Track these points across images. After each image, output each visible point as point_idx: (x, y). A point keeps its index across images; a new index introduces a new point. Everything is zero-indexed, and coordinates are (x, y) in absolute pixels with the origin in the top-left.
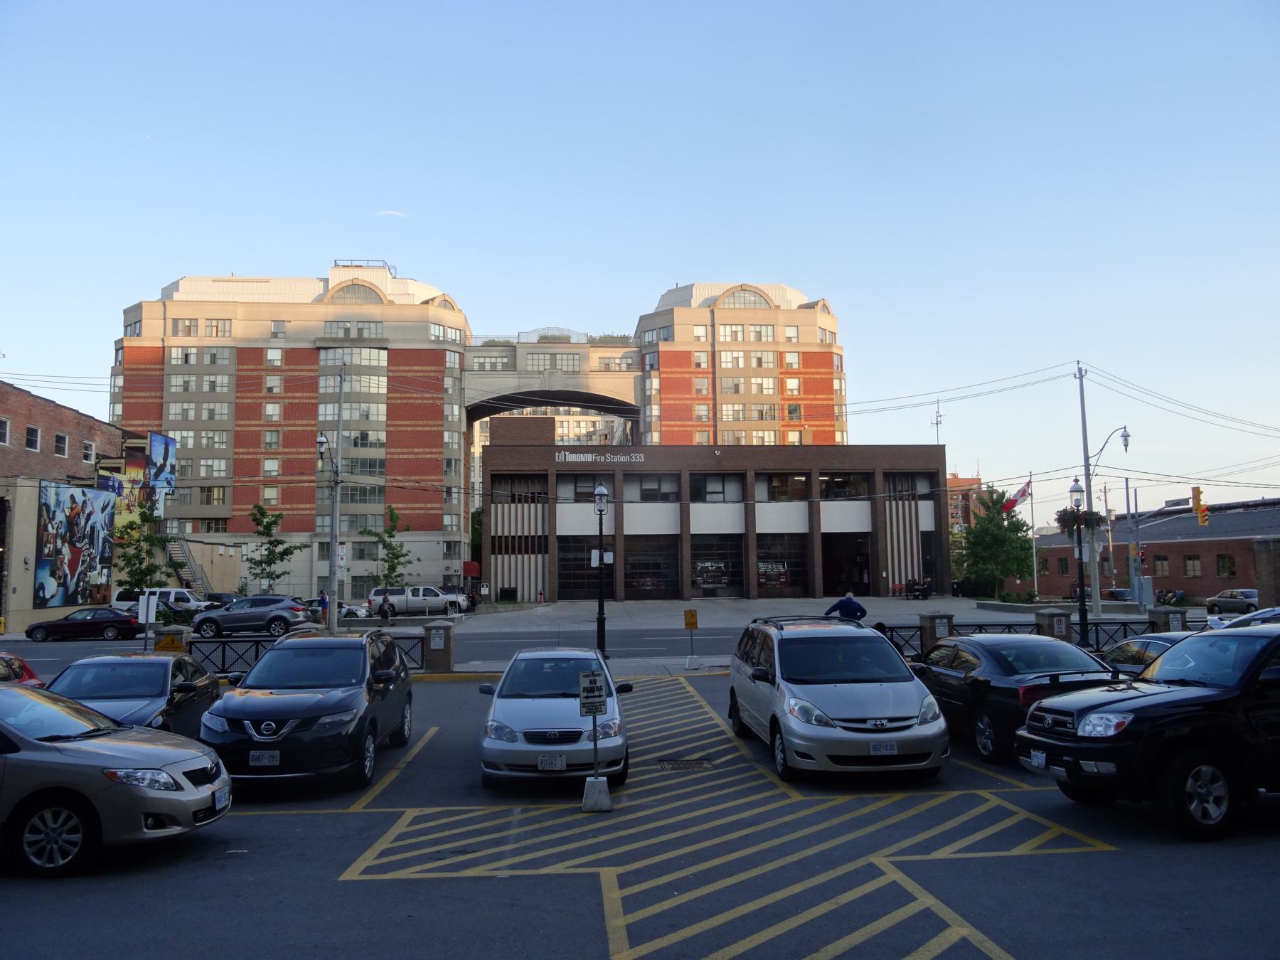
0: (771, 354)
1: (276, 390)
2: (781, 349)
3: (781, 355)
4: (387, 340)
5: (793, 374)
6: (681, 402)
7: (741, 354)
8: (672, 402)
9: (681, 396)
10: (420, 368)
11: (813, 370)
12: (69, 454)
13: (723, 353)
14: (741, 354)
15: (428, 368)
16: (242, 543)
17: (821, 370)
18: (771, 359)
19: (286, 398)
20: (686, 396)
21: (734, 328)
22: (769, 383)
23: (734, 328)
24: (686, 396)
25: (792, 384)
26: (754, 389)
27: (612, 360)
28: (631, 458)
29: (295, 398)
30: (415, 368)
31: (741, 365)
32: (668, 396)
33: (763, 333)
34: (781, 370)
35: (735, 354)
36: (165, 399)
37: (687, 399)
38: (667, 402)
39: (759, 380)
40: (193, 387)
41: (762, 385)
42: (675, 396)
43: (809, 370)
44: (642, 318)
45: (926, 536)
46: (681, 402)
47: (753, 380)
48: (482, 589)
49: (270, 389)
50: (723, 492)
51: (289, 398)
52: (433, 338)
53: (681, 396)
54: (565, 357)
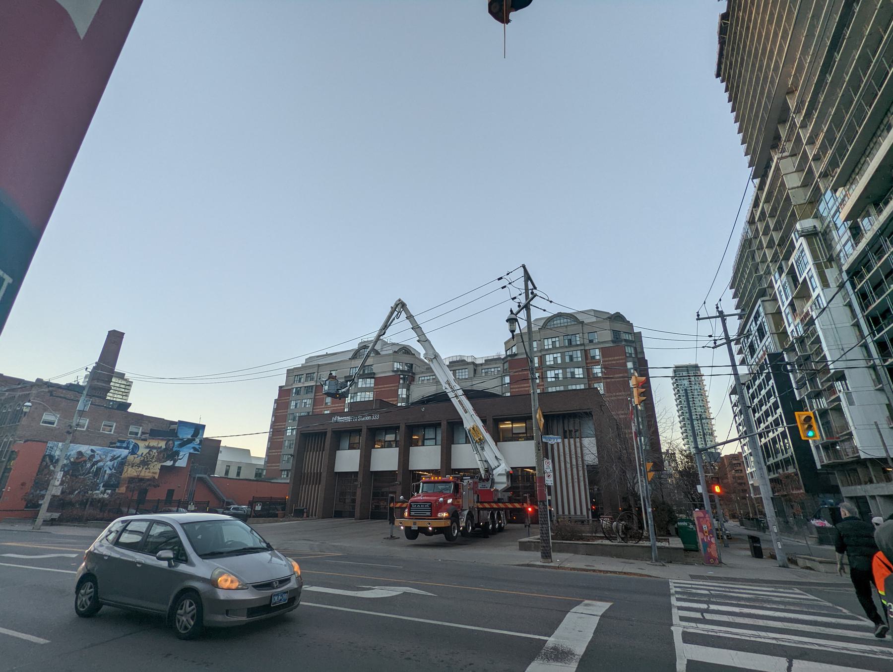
0: (579, 352)
1: (329, 404)
2: (587, 348)
3: (586, 353)
4: (374, 374)
5: (597, 363)
6: (522, 389)
7: (559, 355)
8: (517, 390)
9: (523, 385)
10: (388, 386)
11: (610, 359)
12: (114, 432)
13: (547, 356)
14: (559, 355)
15: (391, 385)
16: (253, 480)
17: (616, 358)
18: (579, 355)
19: (333, 407)
20: (526, 385)
21: (554, 340)
22: (579, 372)
23: (554, 340)
24: (526, 385)
25: (597, 370)
26: (569, 375)
27: (489, 370)
28: (372, 417)
29: (335, 407)
30: (385, 386)
31: (559, 361)
32: (514, 386)
33: (572, 340)
34: (587, 362)
35: (555, 355)
36: (288, 413)
37: (526, 387)
38: (514, 390)
39: (572, 370)
40: (298, 404)
41: (574, 372)
42: (518, 386)
43: (607, 359)
44: (505, 343)
45: (592, 471)
46: (522, 389)
47: (568, 370)
48: (256, 507)
49: (326, 404)
50: (435, 439)
51: (333, 407)
52: (395, 369)
53: (523, 385)
54: (460, 371)
